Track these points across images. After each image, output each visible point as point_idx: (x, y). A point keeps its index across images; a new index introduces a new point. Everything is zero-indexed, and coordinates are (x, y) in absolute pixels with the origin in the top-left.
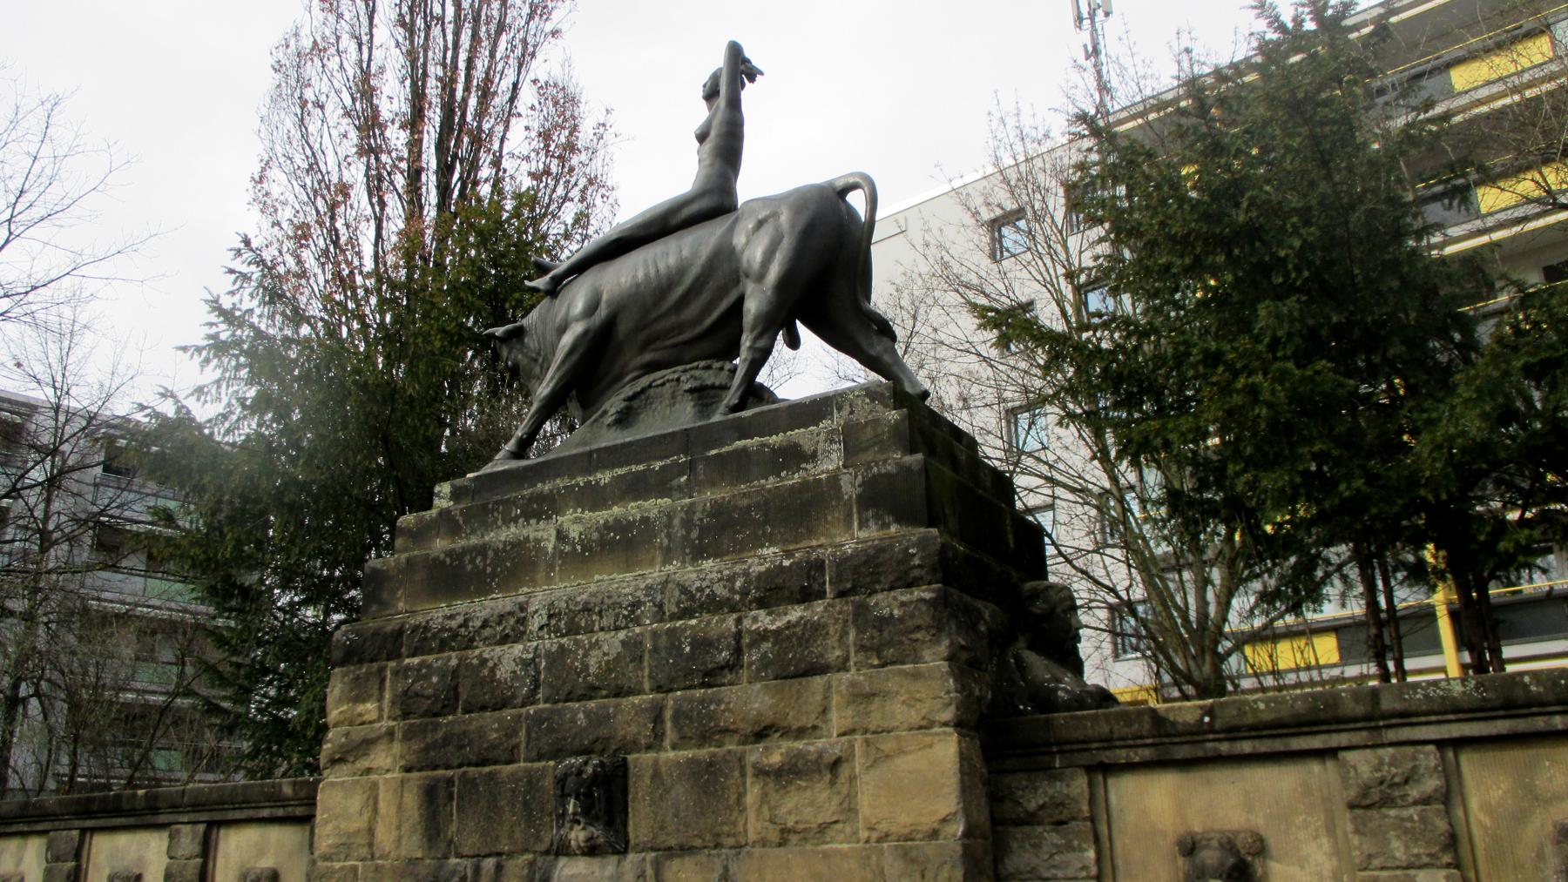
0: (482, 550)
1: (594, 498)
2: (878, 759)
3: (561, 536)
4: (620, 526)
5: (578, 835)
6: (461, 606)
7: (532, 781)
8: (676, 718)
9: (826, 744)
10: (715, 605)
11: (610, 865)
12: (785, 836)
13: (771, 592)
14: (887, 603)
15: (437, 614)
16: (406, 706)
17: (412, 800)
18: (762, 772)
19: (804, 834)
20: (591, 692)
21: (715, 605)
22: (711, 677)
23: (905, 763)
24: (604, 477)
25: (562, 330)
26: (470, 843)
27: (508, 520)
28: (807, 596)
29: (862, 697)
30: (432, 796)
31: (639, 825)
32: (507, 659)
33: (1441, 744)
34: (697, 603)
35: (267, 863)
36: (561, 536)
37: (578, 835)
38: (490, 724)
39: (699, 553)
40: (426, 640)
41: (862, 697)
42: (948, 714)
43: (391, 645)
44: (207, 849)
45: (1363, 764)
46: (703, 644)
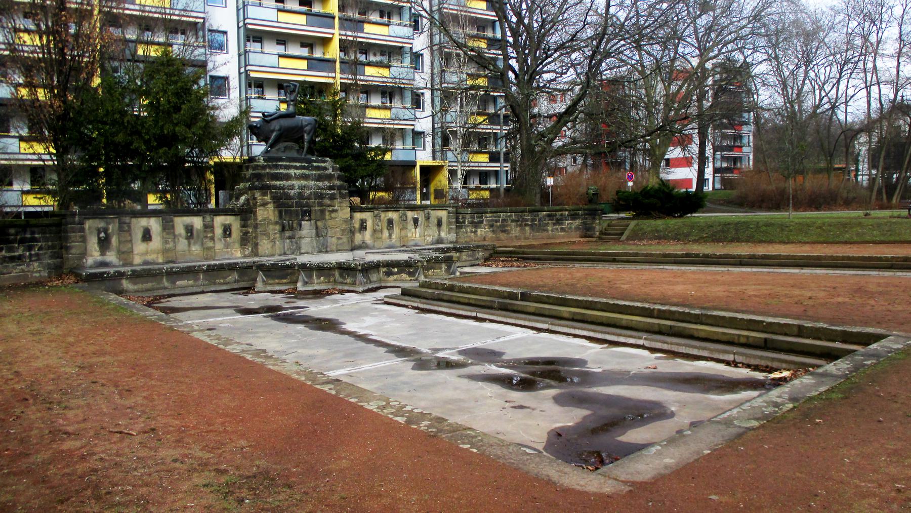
0: (281, 173)
1: (296, 168)
2: (341, 210)
3: (295, 174)
4: (305, 174)
5: (307, 218)
6: (281, 183)
7: (297, 211)
8: (318, 203)
9: (336, 208)
10: (322, 189)
11: (309, 222)
12: (332, 218)
13: (331, 188)
14: (344, 192)
15: (278, 183)
16: (273, 198)
17: (276, 213)
18: (329, 211)
19: (335, 218)
20: (305, 199)
21: (322, 189)
22: (322, 198)
23: (344, 211)
24: (298, 164)
25: (273, 131)
26: (288, 219)
27: (281, 168)
28: (334, 189)
29: (340, 203)
30: (280, 213)
31: (313, 217)
32: (292, 192)
34: (319, 188)
35: (227, 222)
36: (295, 174)
37: (307, 218)
38: (290, 202)
39: (317, 181)
40: (275, 187)
41: (340, 203)
43: (269, 187)
44: (213, 221)
45: (376, 212)
46: (321, 194)
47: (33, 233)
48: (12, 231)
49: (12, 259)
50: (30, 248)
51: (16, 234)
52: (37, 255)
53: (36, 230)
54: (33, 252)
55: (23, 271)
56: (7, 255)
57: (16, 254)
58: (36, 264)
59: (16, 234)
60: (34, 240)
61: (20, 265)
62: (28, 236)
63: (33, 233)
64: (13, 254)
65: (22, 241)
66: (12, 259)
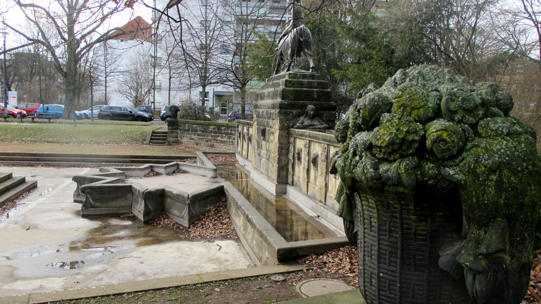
33: (310, 141)
42: (278, 128)
47: (231, 130)
48: (223, 128)
49: (222, 142)
50: (229, 138)
51: (225, 130)
52: (232, 142)
53: (233, 129)
54: (231, 140)
55: (226, 149)
56: (221, 139)
57: (224, 140)
58: (232, 146)
59: (225, 130)
60: (231, 134)
61: (225, 145)
62: (230, 132)
63: (231, 130)
64: (223, 139)
65: (226, 134)
66: (222, 142)
